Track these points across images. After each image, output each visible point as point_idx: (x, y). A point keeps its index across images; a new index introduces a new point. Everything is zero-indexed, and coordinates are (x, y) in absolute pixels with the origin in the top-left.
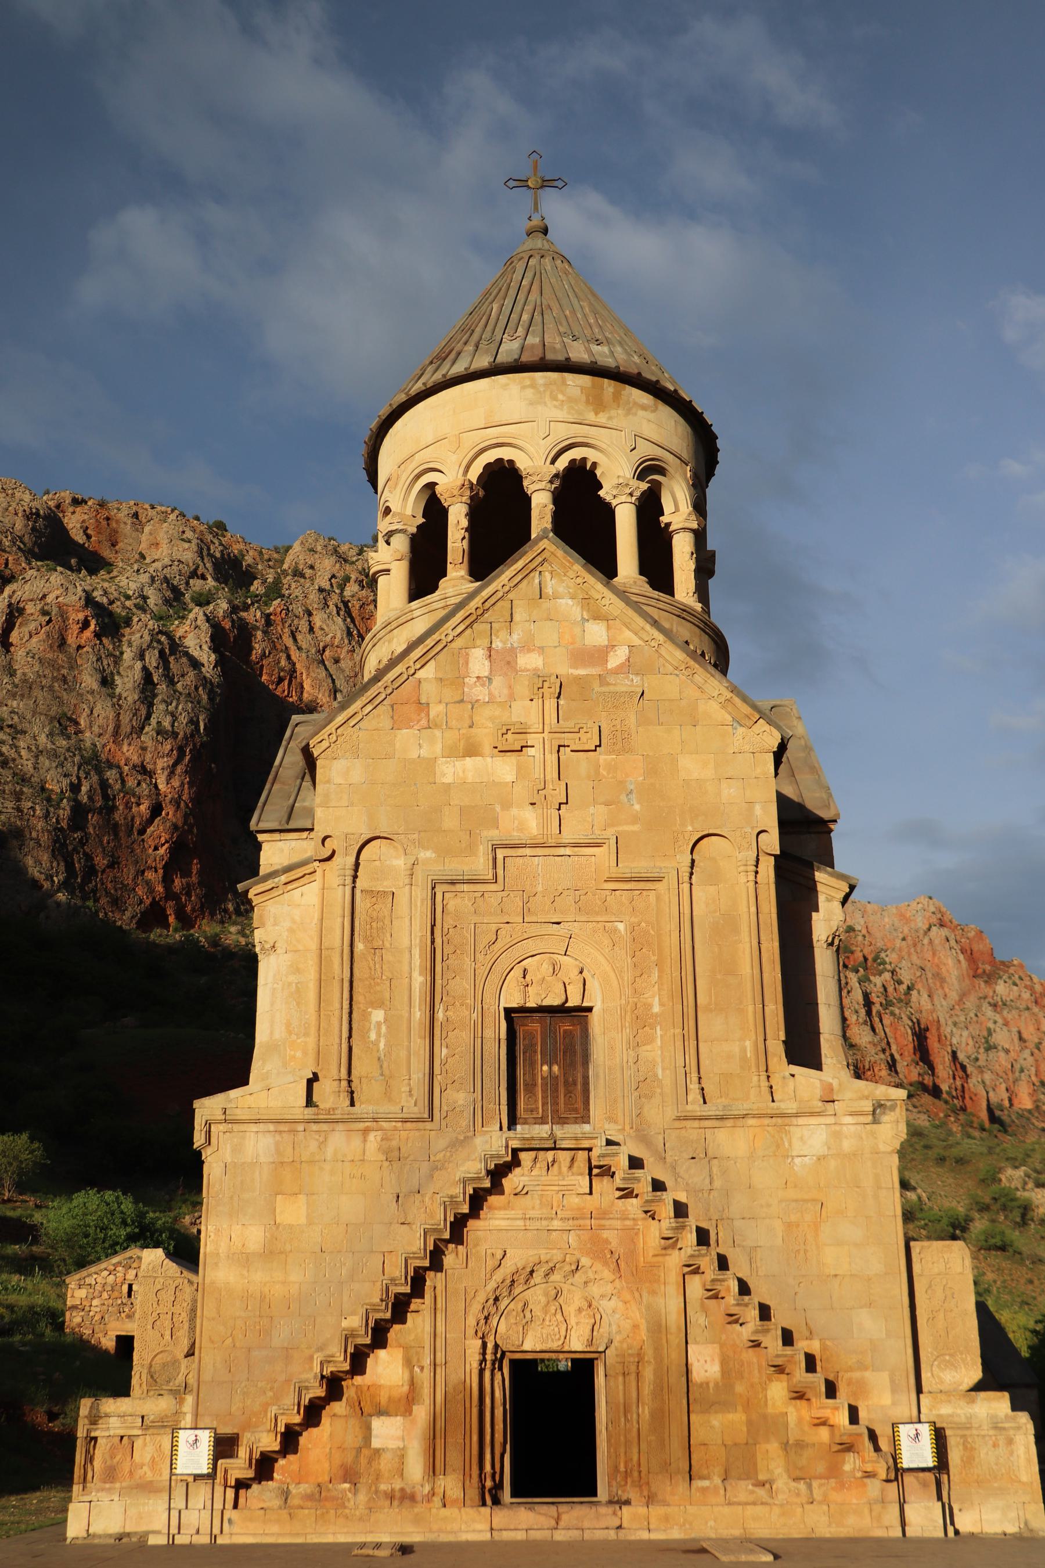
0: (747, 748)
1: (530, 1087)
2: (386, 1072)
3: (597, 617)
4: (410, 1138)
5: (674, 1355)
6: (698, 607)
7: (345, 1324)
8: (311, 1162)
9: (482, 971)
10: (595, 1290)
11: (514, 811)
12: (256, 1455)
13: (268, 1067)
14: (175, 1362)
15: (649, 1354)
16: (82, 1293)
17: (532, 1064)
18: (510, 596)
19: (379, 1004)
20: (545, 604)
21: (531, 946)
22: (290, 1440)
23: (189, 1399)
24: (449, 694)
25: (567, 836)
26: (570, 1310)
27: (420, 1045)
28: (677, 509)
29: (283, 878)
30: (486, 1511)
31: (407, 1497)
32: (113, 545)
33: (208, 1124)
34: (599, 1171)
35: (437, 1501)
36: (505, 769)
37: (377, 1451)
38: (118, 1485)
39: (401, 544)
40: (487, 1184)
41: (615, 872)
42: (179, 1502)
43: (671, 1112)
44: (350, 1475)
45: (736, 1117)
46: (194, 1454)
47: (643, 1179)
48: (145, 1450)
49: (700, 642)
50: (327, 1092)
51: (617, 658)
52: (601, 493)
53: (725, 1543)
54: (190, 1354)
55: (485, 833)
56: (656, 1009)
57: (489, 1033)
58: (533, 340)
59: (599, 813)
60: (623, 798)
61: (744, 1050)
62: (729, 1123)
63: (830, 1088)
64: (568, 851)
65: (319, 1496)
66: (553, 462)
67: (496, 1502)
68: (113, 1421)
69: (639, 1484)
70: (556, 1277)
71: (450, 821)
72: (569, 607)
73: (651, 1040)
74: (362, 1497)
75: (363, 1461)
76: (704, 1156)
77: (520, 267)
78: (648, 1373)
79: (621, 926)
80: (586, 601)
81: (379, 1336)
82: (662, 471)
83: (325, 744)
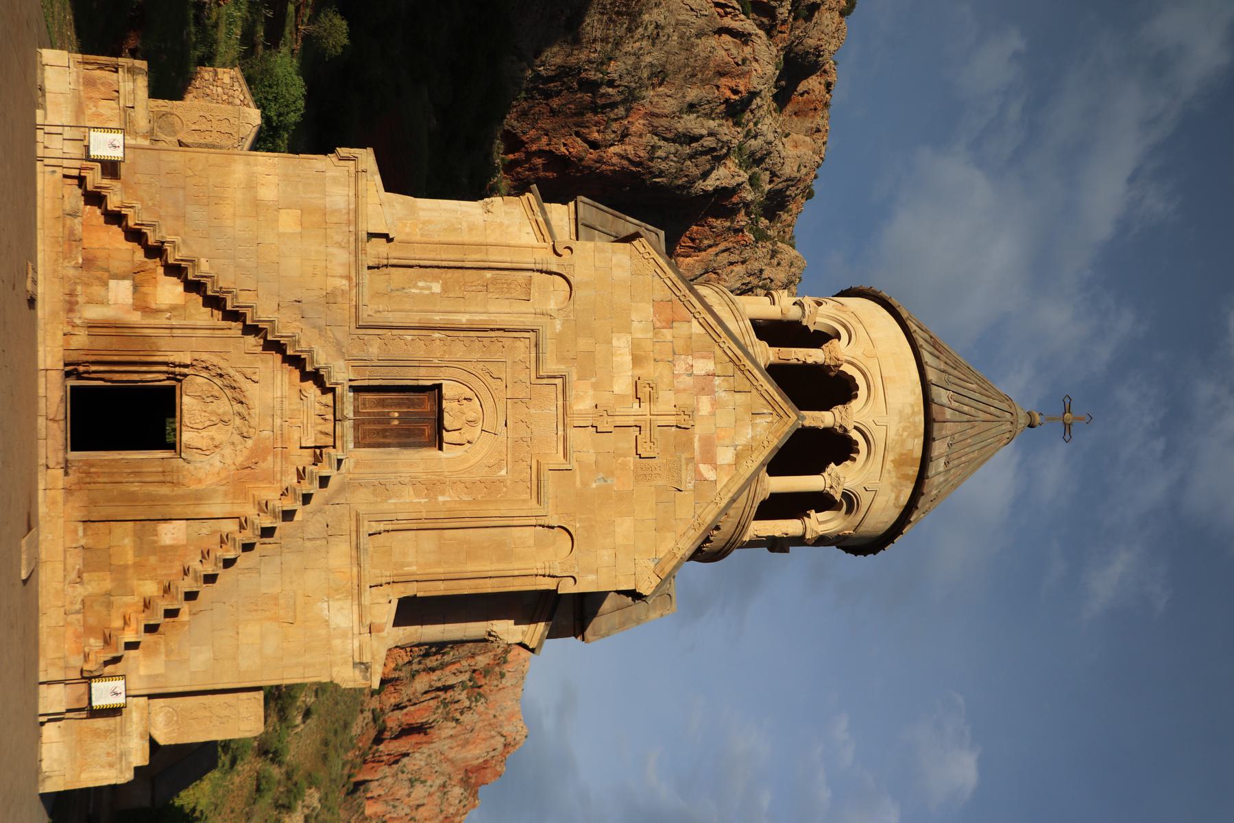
0: (639, 569)
1: (382, 403)
2: (394, 294)
3: (738, 456)
4: (343, 311)
5: (178, 510)
6: (746, 538)
7: (203, 260)
8: (326, 236)
9: (470, 367)
10: (228, 451)
11: (591, 392)
12: (104, 192)
13: (398, 207)
14: (175, 133)
15: (179, 491)
16: (227, 80)
17: (399, 405)
18: (754, 391)
19: (445, 289)
20: (748, 417)
21: (488, 404)
22: (115, 218)
23: (146, 143)
24: (680, 344)
25: (572, 432)
26: (213, 432)
27: (415, 319)
28: (821, 523)
29: (540, 219)
31: (71, 306)
32: (795, 113)
33: (355, 159)
34: (318, 454)
35: (69, 329)
36: (623, 385)
37: (106, 284)
38: (81, 88)
39: (794, 313)
40: (309, 369)
41: (544, 468)
42: (68, 133)
43: (362, 509)
44: (88, 263)
45: (358, 558)
46: (105, 145)
47: (311, 487)
48: (108, 110)
49: (719, 539)
50: (378, 249)
51: (707, 471)
52: (832, 465)
53: (34, 545)
54: (181, 144)
55: (574, 370)
56: (441, 499)
57: (423, 372)
58: (949, 414)
59: (590, 457)
60: (601, 475)
61: (410, 565)
62: (354, 553)
63: (380, 630)
64: (561, 433)
65: (72, 239)
66: (856, 428)
67: (68, 375)
68: (130, 85)
69: (81, 484)
70: (238, 421)
71: (583, 344)
72: (746, 435)
73: (418, 496)
74: (71, 272)
75: (99, 274)
76: (329, 534)
77: (1004, 406)
78: (164, 490)
79: (503, 472)
80: (750, 449)
81: (194, 286)
82: (849, 511)
83: (642, 249)
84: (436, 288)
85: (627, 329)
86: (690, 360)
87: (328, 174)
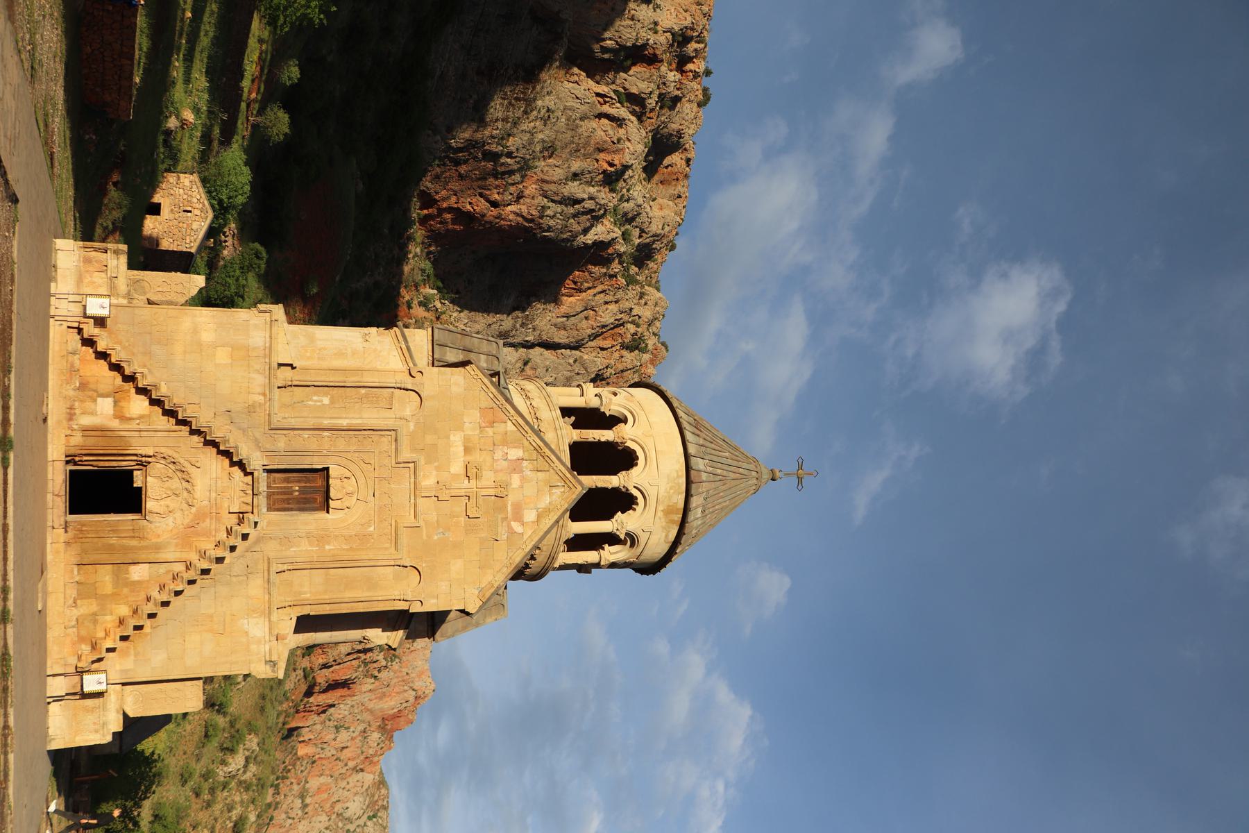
1: (287, 480)
3: (539, 516)
4: (261, 418)
5: (143, 556)
6: (556, 565)
7: (163, 384)
8: (249, 366)
9: (349, 456)
10: (178, 514)
11: (434, 473)
14: (145, 293)
15: (143, 543)
17: (299, 481)
19: (332, 402)
20: (547, 489)
21: (362, 481)
22: (102, 356)
23: (125, 302)
24: (498, 438)
25: (420, 501)
26: (168, 501)
27: (311, 423)
28: (611, 553)
29: (404, 346)
30: (63, 458)
31: (71, 416)
33: (270, 312)
34: (241, 517)
35: (69, 432)
36: (457, 467)
39: (595, 403)
40: (235, 459)
41: (401, 526)
42: (71, 298)
43: (272, 555)
44: (83, 386)
46: (96, 307)
47: (237, 541)
48: (100, 278)
49: (535, 566)
50: (286, 373)
51: (517, 527)
53: (45, 584)
54: (150, 302)
56: (327, 547)
57: (316, 459)
58: (704, 476)
59: (433, 517)
63: (284, 638)
65: (73, 370)
67: (67, 462)
68: (115, 262)
69: (76, 537)
70: (185, 494)
71: (430, 439)
72: (545, 501)
73: (311, 545)
74: (72, 393)
75: (90, 393)
76: (249, 572)
77: (752, 467)
78: (134, 543)
79: (372, 529)
80: (548, 510)
81: (155, 402)
82: (632, 545)
84: (326, 401)
85: (460, 428)
86: (505, 449)
87: (252, 322)
